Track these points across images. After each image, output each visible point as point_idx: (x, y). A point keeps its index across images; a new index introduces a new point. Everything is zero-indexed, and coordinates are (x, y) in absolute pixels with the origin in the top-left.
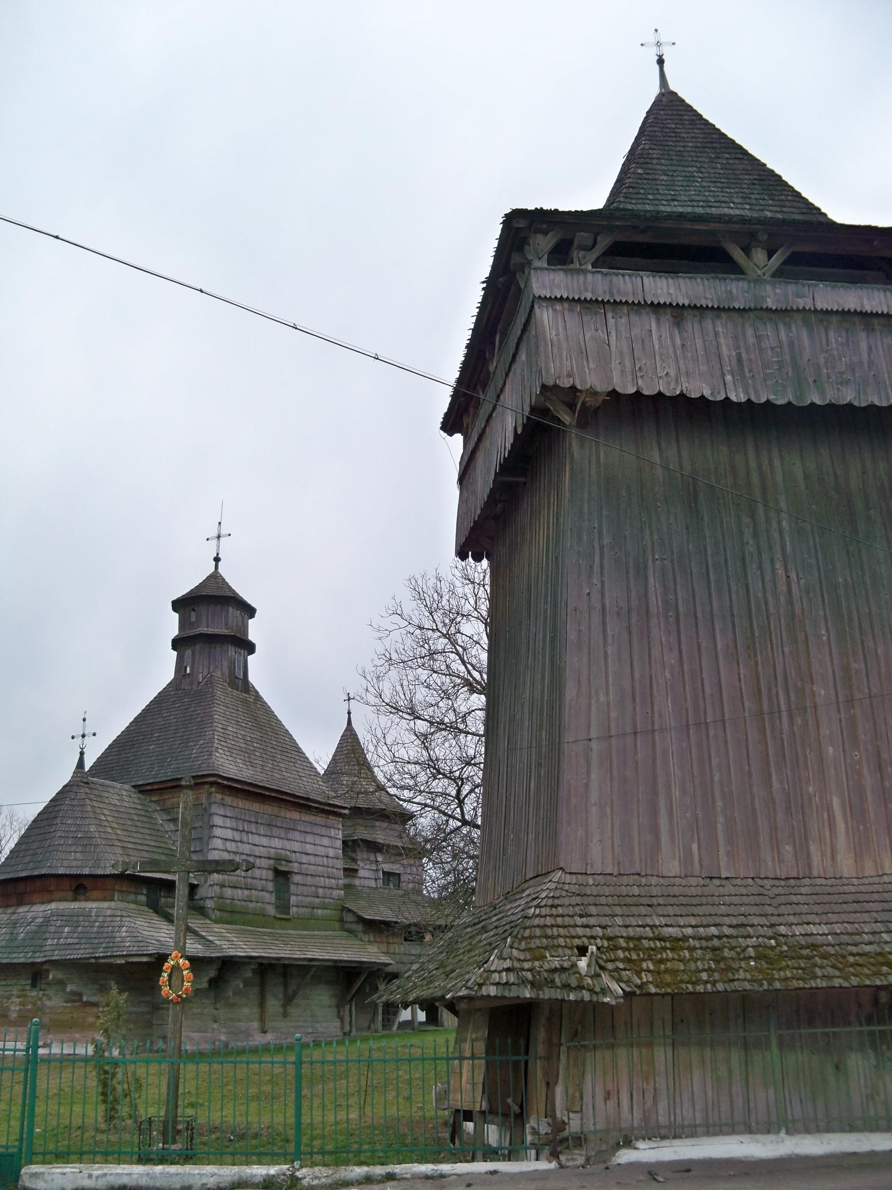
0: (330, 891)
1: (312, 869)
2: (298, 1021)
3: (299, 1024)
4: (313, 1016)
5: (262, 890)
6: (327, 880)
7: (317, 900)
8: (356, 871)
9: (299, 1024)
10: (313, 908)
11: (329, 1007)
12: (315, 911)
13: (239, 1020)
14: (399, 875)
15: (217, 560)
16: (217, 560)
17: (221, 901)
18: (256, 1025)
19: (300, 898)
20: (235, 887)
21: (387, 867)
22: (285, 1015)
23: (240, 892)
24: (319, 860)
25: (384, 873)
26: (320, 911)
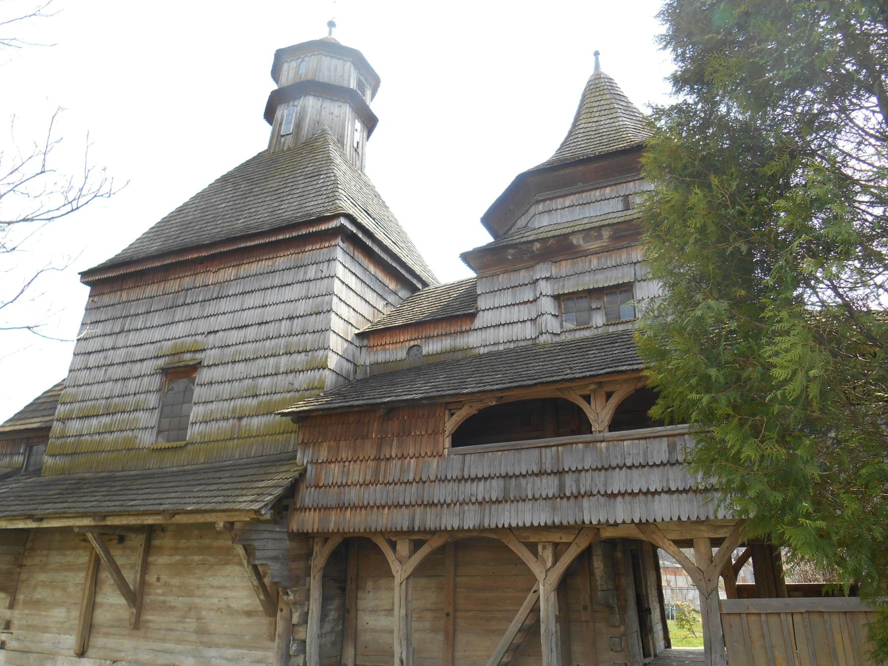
0: (291, 377)
1: (249, 350)
2: (163, 640)
3: (167, 646)
4: (202, 631)
5: (136, 410)
6: (284, 360)
7: (254, 402)
8: (473, 316)
9: (167, 646)
10: (240, 418)
11: (249, 614)
12: (244, 422)
13: (45, 629)
14: (626, 289)
15: (331, 24)
16: (331, 24)
17: (59, 441)
18: (71, 641)
19: (213, 406)
20: (87, 417)
21: (570, 286)
22: (137, 624)
23: (94, 422)
24: (251, 333)
25: (557, 298)
26: (256, 422)
